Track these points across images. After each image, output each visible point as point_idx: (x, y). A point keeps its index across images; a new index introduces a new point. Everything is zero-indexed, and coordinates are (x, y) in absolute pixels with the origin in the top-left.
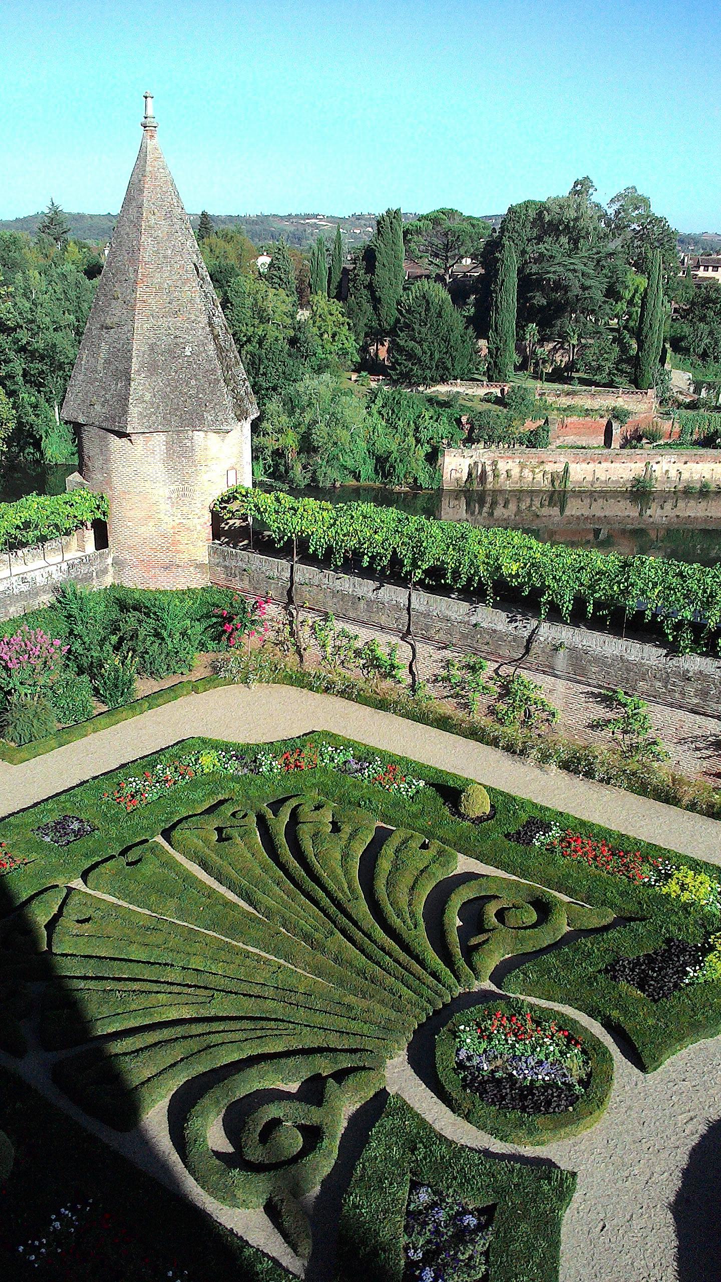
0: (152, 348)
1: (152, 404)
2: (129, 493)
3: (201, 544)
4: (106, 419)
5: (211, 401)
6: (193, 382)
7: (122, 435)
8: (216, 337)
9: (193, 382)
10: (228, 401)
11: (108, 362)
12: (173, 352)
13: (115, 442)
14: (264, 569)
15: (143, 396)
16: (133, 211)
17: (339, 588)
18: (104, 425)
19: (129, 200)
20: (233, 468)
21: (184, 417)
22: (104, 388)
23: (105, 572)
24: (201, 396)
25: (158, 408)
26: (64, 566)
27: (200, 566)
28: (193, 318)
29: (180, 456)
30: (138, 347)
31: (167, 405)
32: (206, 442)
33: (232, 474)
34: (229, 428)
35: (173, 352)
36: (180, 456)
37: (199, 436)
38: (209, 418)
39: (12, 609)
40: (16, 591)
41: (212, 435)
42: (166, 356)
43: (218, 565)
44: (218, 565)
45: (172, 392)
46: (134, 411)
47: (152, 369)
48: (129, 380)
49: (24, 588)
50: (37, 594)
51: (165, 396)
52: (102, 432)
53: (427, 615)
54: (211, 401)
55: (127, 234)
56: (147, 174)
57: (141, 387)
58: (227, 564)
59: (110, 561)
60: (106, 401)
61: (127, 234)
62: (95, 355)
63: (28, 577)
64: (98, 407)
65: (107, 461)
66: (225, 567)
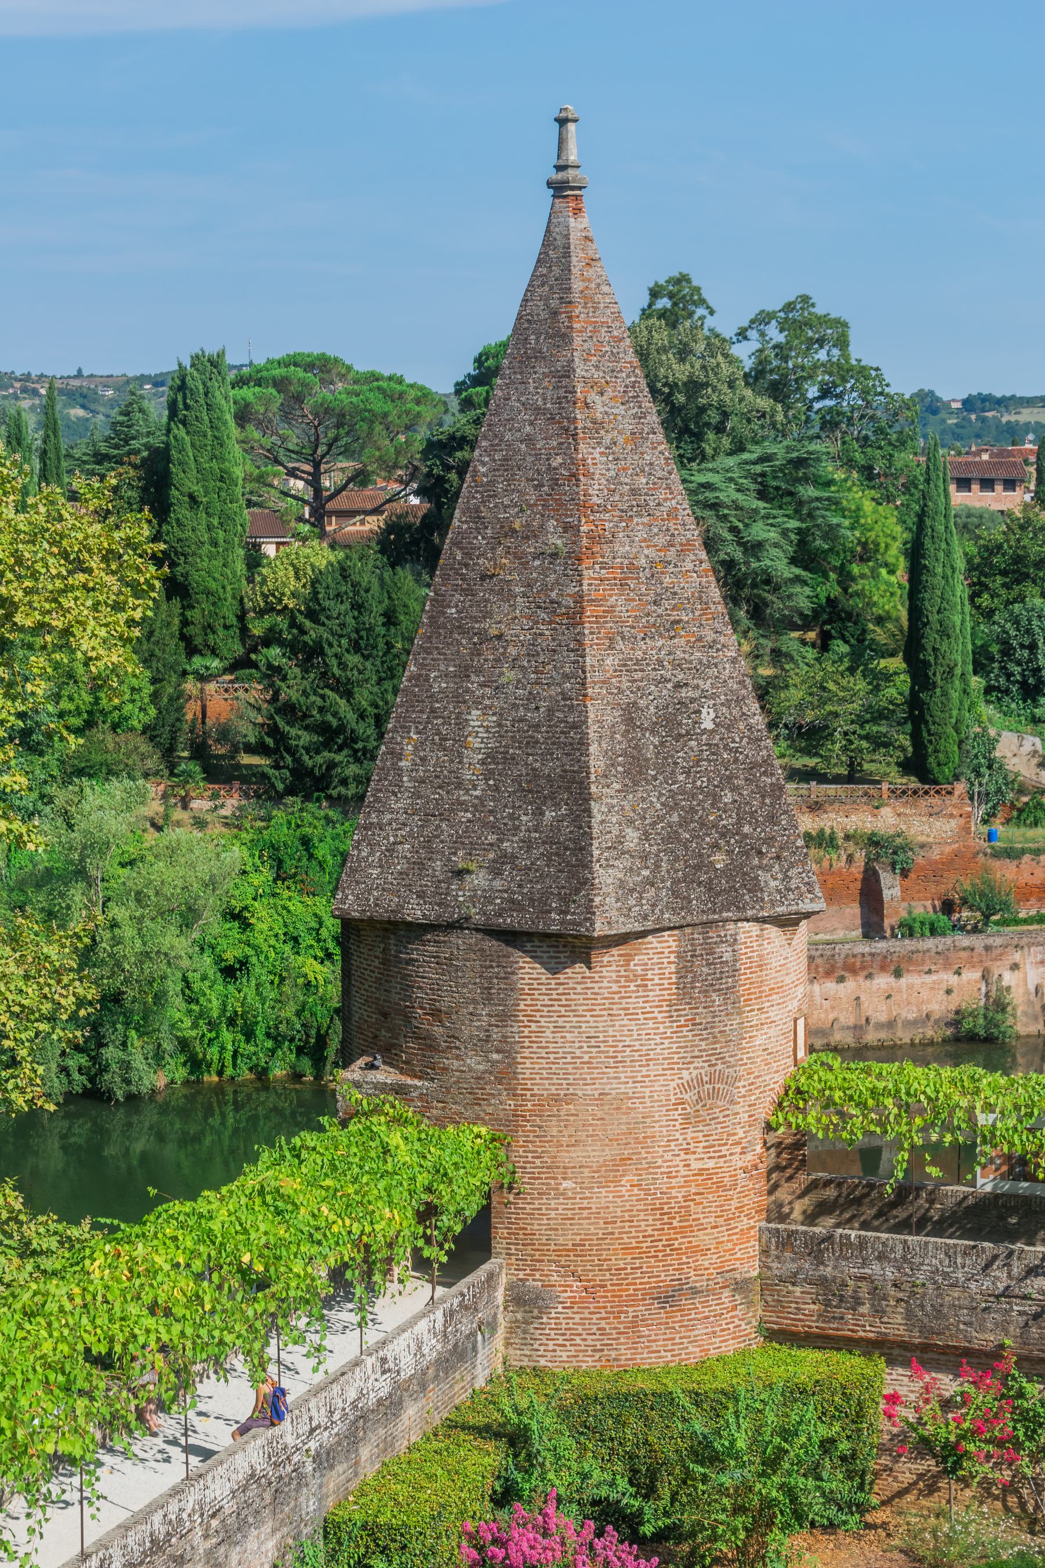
0: (630, 714)
1: (645, 857)
2: (569, 1099)
3: (745, 1223)
5: (770, 840)
6: (728, 797)
9: (728, 797)
12: (674, 722)
13: (528, 971)
15: (620, 839)
18: (509, 921)
22: (493, 828)
24: (746, 829)
25: (658, 866)
27: (740, 1286)
28: (710, 636)
30: (600, 715)
31: (677, 859)
35: (674, 722)
37: (748, 930)
38: (773, 884)
45: (684, 823)
47: (635, 770)
52: (491, 945)
54: (770, 840)
56: (576, 296)
57: (615, 815)
58: (828, 1271)
59: (500, 1295)
60: (505, 858)
61: (529, 440)
62: (454, 744)
64: (479, 880)
65: (505, 1017)
66: (823, 1282)
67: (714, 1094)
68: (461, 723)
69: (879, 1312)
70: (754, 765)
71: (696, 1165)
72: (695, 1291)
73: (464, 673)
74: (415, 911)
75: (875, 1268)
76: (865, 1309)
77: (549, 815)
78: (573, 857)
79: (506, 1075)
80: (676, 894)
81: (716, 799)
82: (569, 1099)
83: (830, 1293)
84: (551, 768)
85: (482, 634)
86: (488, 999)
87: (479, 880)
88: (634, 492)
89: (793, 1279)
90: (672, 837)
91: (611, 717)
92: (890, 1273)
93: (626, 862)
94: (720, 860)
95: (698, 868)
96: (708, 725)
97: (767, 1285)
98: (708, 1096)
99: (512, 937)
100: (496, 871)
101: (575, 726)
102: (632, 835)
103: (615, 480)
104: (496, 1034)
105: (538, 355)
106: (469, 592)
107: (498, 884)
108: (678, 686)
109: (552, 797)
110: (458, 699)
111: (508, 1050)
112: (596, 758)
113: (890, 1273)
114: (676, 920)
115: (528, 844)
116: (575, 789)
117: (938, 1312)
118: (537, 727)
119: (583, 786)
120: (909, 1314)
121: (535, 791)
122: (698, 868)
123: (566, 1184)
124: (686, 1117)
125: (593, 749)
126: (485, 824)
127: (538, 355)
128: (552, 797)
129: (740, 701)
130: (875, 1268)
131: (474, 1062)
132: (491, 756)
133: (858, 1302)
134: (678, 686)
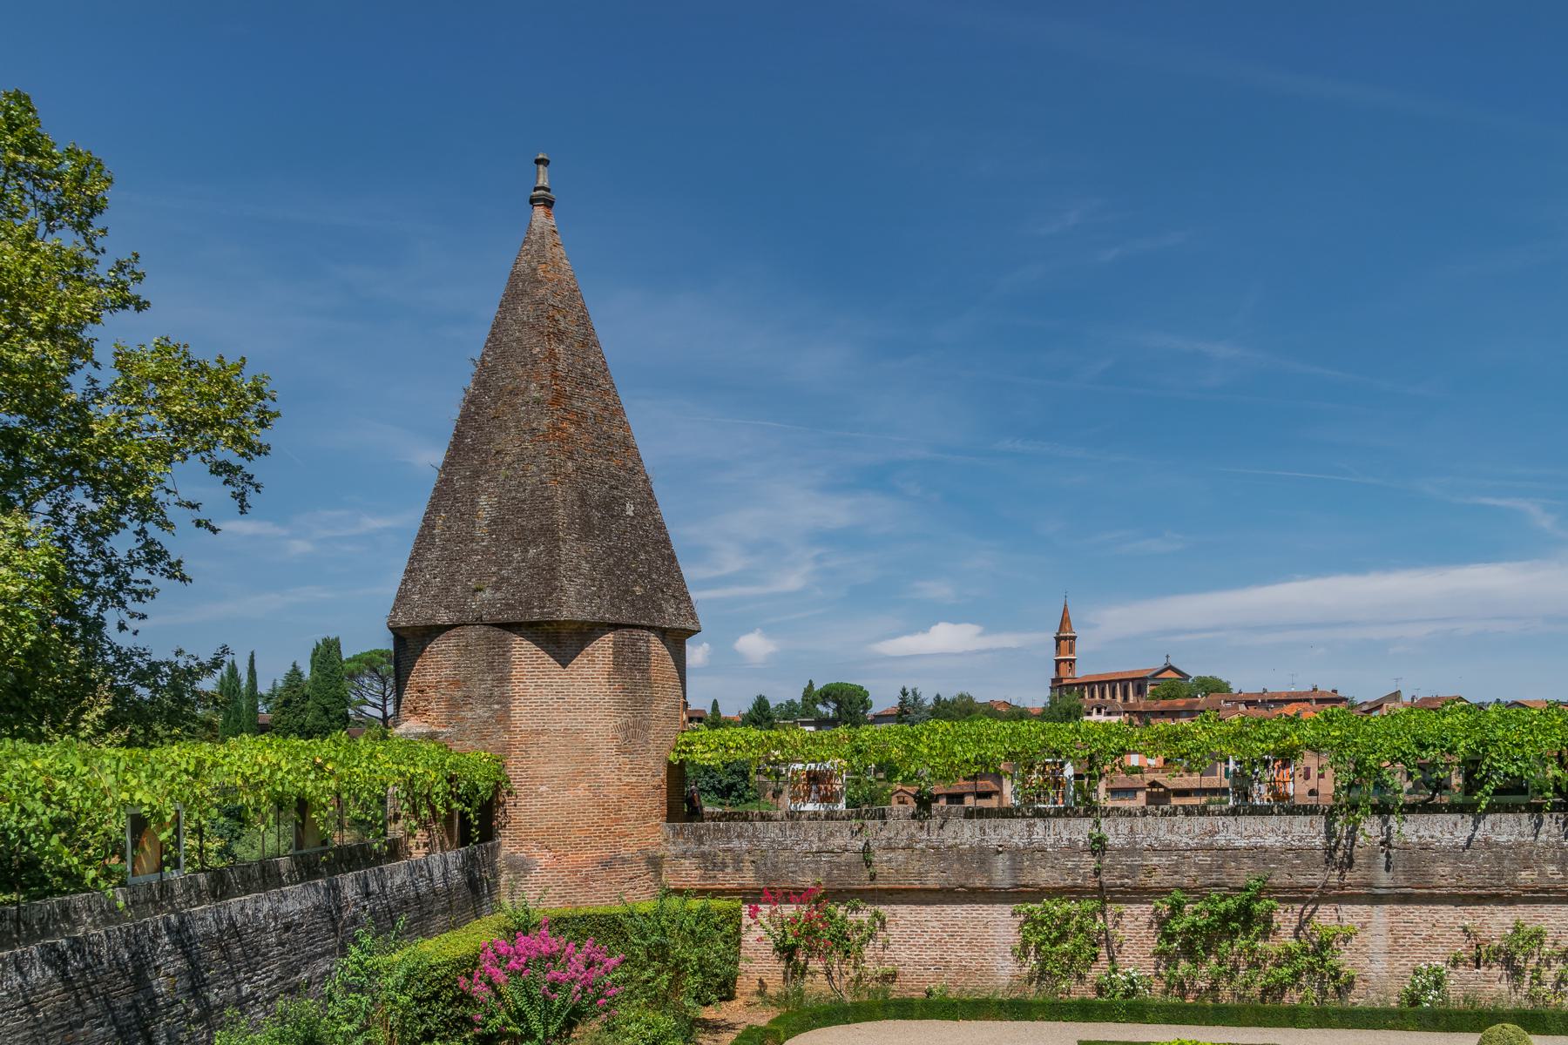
0: (583, 497)
1: (593, 580)
11: (496, 523)
15: (577, 567)
17: (950, 842)
18: (505, 617)
22: (495, 563)
45: (617, 564)
47: (587, 530)
52: (494, 633)
53: (1131, 850)
58: (705, 848)
60: (503, 579)
61: (519, 340)
64: (487, 594)
65: (503, 680)
66: (703, 855)
68: (474, 504)
69: (738, 870)
73: (476, 474)
74: (443, 618)
75: (735, 844)
76: (729, 870)
77: (532, 552)
78: (547, 575)
83: (708, 862)
85: (487, 452)
86: (492, 669)
89: (684, 855)
90: (609, 572)
91: (572, 496)
92: (745, 845)
94: (638, 590)
95: (626, 592)
98: (632, 736)
100: (497, 588)
101: (548, 499)
104: (497, 692)
105: (524, 293)
106: (479, 428)
107: (498, 595)
109: (534, 541)
110: (473, 491)
111: (505, 702)
113: (745, 845)
117: (775, 866)
118: (524, 501)
120: (757, 869)
121: (523, 539)
122: (626, 592)
123: (543, 788)
124: (619, 747)
126: (489, 562)
127: (524, 293)
128: (534, 541)
130: (735, 844)
131: (482, 712)
132: (494, 521)
133: (725, 865)
134: (611, 487)
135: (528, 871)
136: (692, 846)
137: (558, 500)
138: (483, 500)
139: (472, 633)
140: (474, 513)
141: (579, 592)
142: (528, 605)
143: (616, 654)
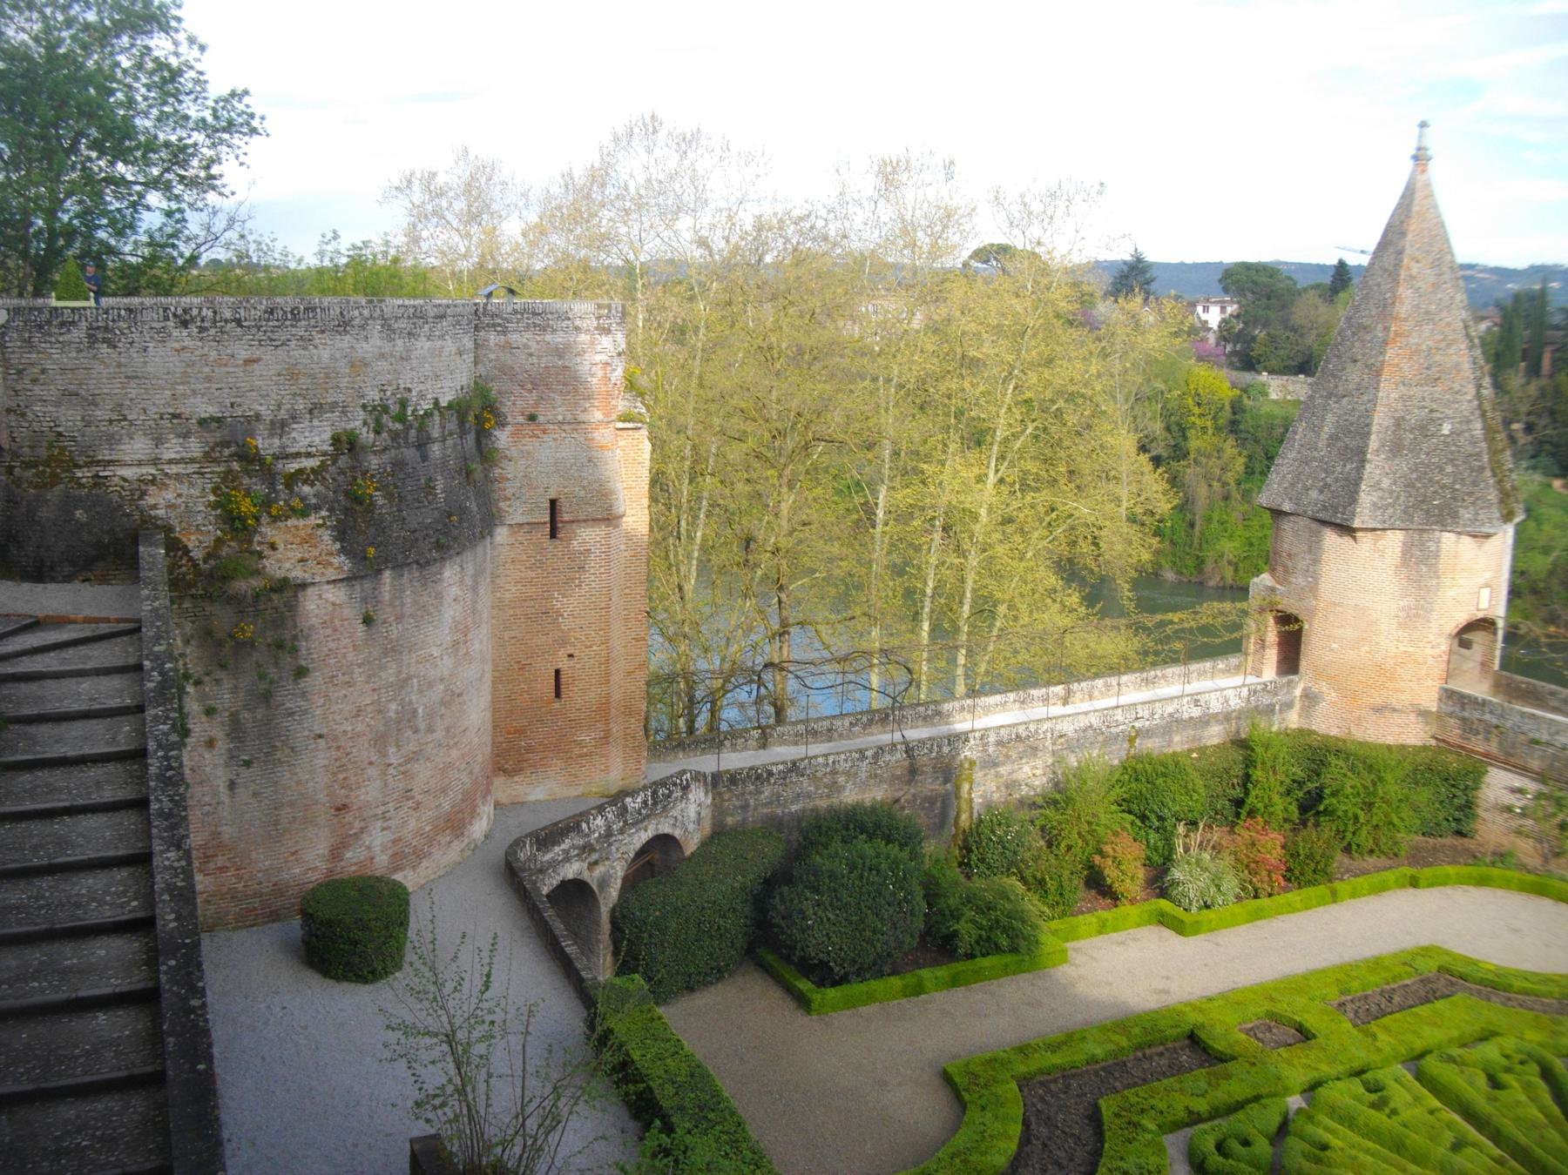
0: (1399, 423)
2: (1340, 605)
3: (1430, 683)
4: (1325, 508)
6: (1449, 469)
7: (1347, 530)
8: (1483, 415)
9: (1449, 469)
10: (1493, 496)
11: (1334, 438)
13: (1330, 538)
14: (1526, 728)
16: (1388, 260)
18: (1321, 515)
19: (1383, 245)
20: (1487, 585)
21: (1431, 510)
22: (1326, 471)
23: (1289, 705)
26: (1245, 692)
27: (1423, 713)
28: (1457, 387)
29: (1420, 563)
30: (1380, 420)
32: (1452, 545)
33: (1485, 593)
34: (1486, 530)
35: (1425, 429)
36: (1420, 563)
37: (1448, 539)
39: (1177, 739)
40: (1186, 716)
41: (1466, 540)
42: (1413, 434)
43: (1451, 715)
44: (1451, 715)
46: (1366, 498)
47: (1396, 449)
48: (1363, 462)
49: (1196, 712)
50: (1207, 723)
51: (1410, 485)
52: (1314, 526)
54: (1470, 494)
55: (1379, 285)
57: (1378, 471)
58: (1466, 714)
59: (1298, 692)
60: (1327, 486)
61: (1379, 285)
62: (1316, 429)
63: (1203, 698)
64: (1314, 494)
65: (1316, 561)
66: (1464, 719)
67: (1417, 615)
68: (1323, 420)
70: (1471, 455)
71: (1402, 649)
72: (1394, 710)
74: (1286, 507)
79: (1313, 589)
80: (1405, 512)
81: (1441, 470)
82: (1340, 605)
84: (1353, 444)
86: (1310, 551)
87: (1314, 494)
88: (1427, 313)
92: (1494, 721)
93: (1380, 494)
96: (1446, 432)
97: (1439, 716)
98: (1413, 617)
99: (1324, 523)
100: (1321, 492)
102: (1386, 483)
103: (1417, 306)
106: (1339, 357)
108: (1432, 411)
111: (1316, 577)
112: (1374, 443)
114: (1403, 526)
115: (1337, 480)
116: (1360, 456)
119: (1364, 454)
120: (1500, 744)
125: (1373, 437)
129: (1469, 422)
130: (1487, 717)
133: (1478, 733)
134: (1432, 411)
135: (1317, 703)
136: (1457, 709)
137: (1374, 428)
138: (1330, 418)
139: (1303, 522)
140: (1321, 428)
141: (1374, 504)
142: (1335, 508)
143: (1404, 553)
